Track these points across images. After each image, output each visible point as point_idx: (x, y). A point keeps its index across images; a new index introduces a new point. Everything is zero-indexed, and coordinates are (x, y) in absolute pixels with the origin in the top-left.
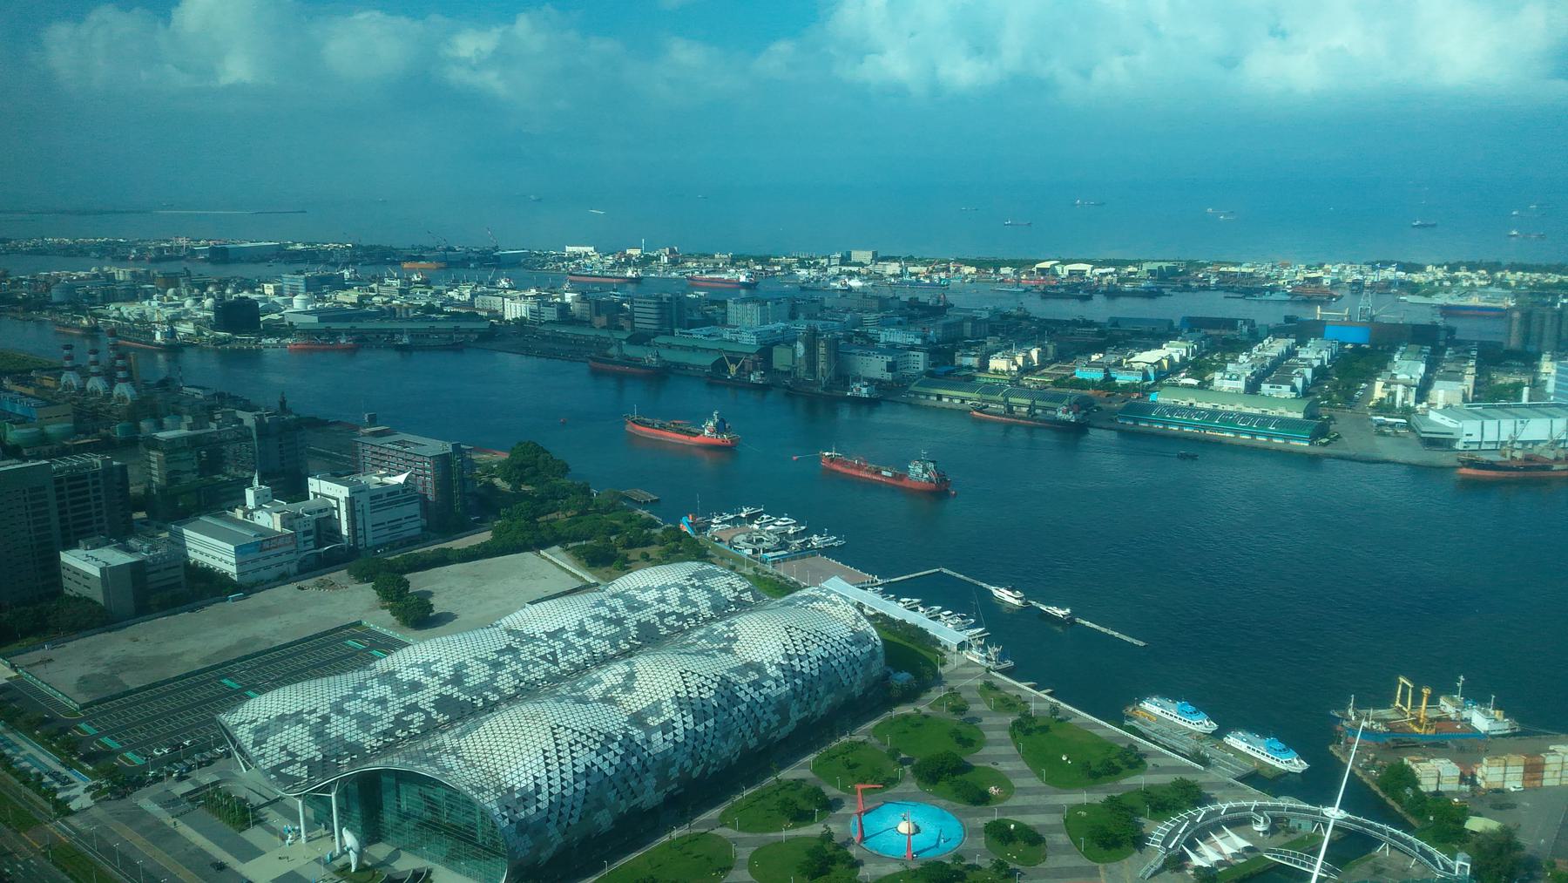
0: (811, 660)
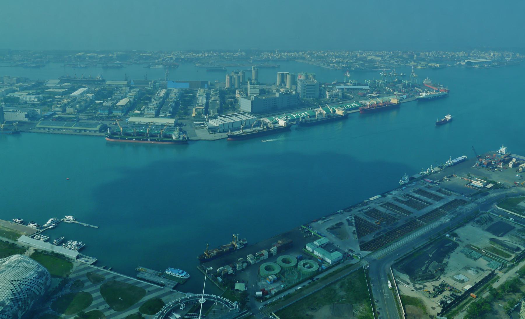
0: (23, 292)
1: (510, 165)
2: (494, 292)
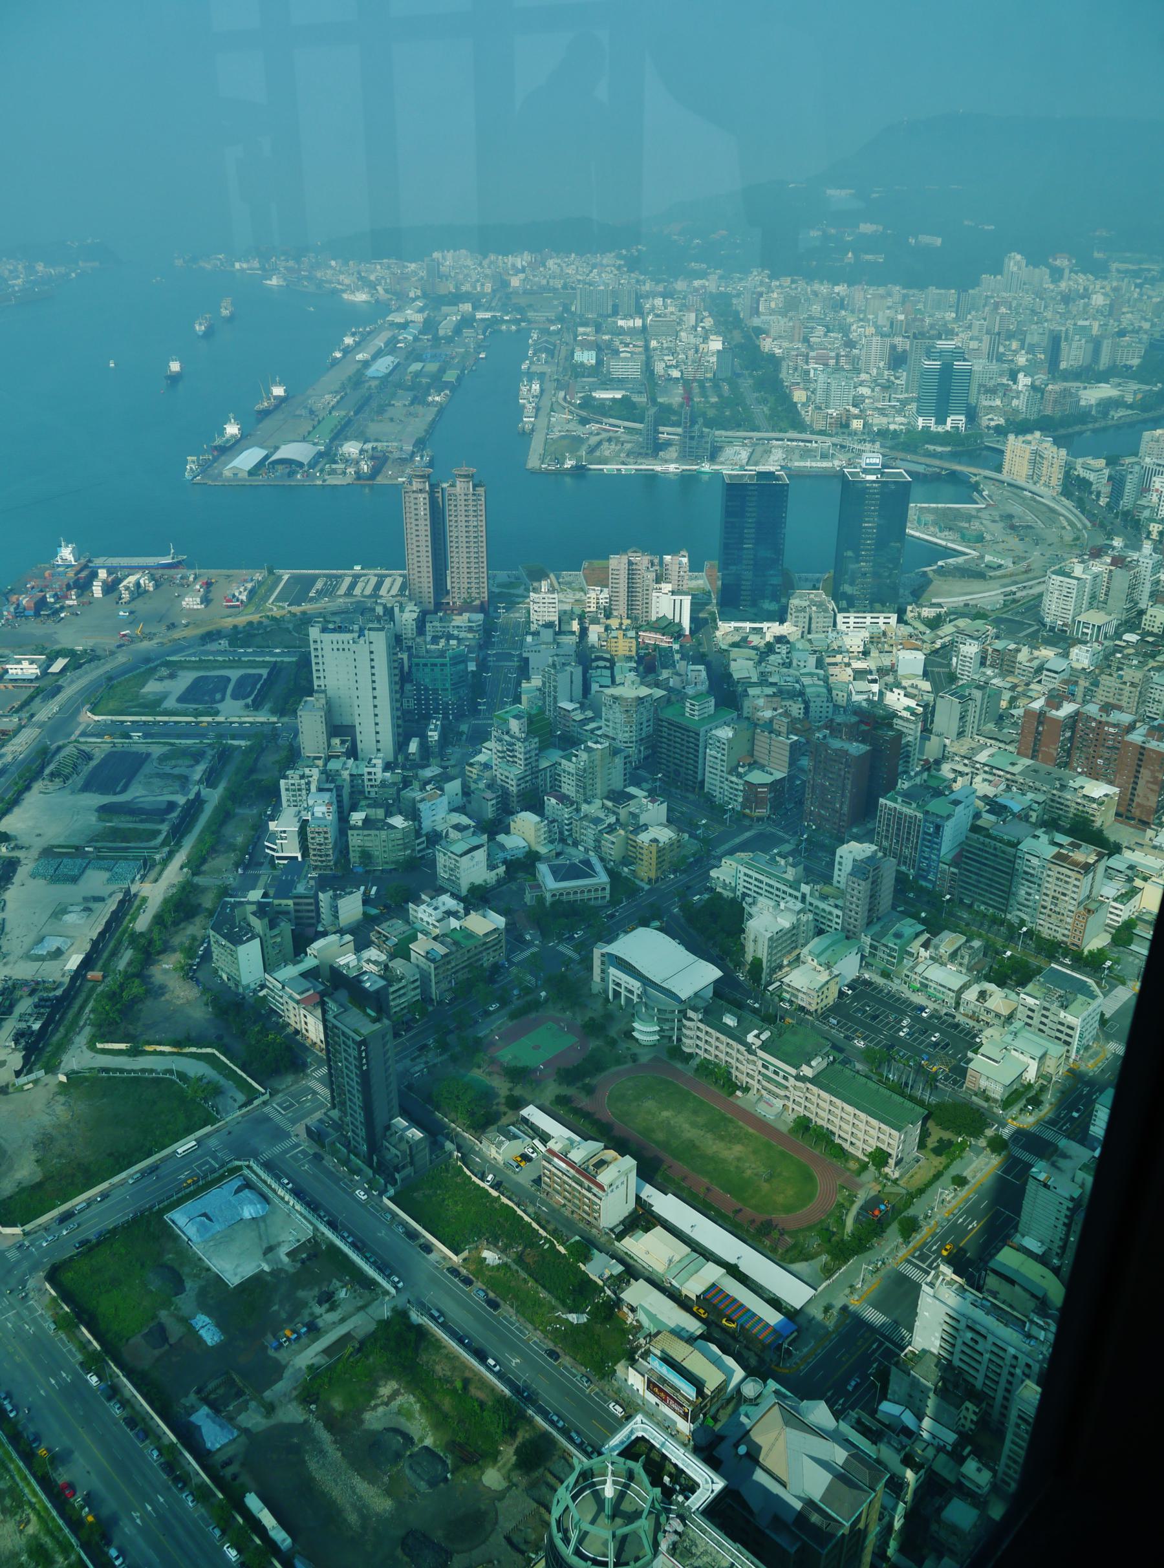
1: (97, 590)
2: (143, 941)
